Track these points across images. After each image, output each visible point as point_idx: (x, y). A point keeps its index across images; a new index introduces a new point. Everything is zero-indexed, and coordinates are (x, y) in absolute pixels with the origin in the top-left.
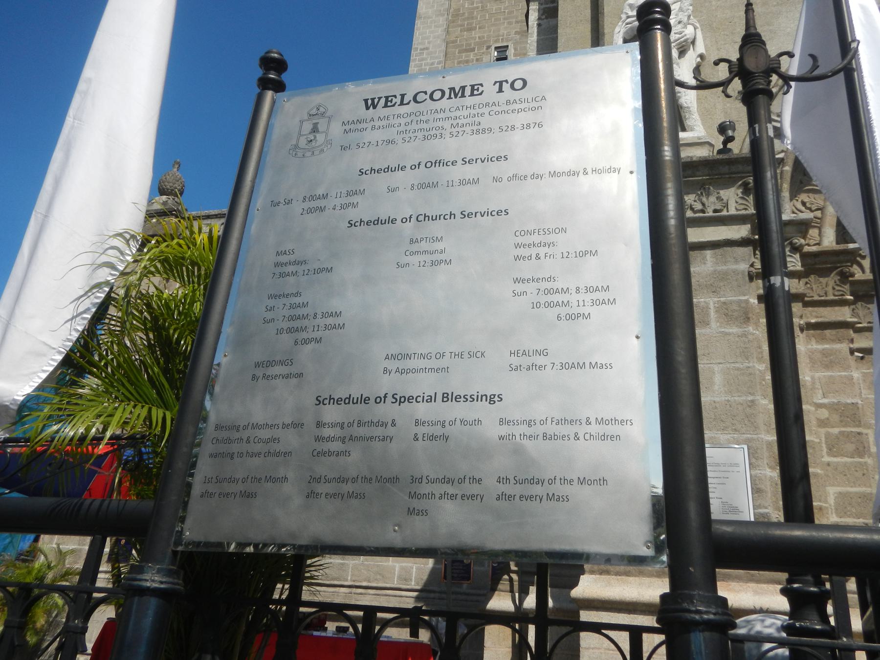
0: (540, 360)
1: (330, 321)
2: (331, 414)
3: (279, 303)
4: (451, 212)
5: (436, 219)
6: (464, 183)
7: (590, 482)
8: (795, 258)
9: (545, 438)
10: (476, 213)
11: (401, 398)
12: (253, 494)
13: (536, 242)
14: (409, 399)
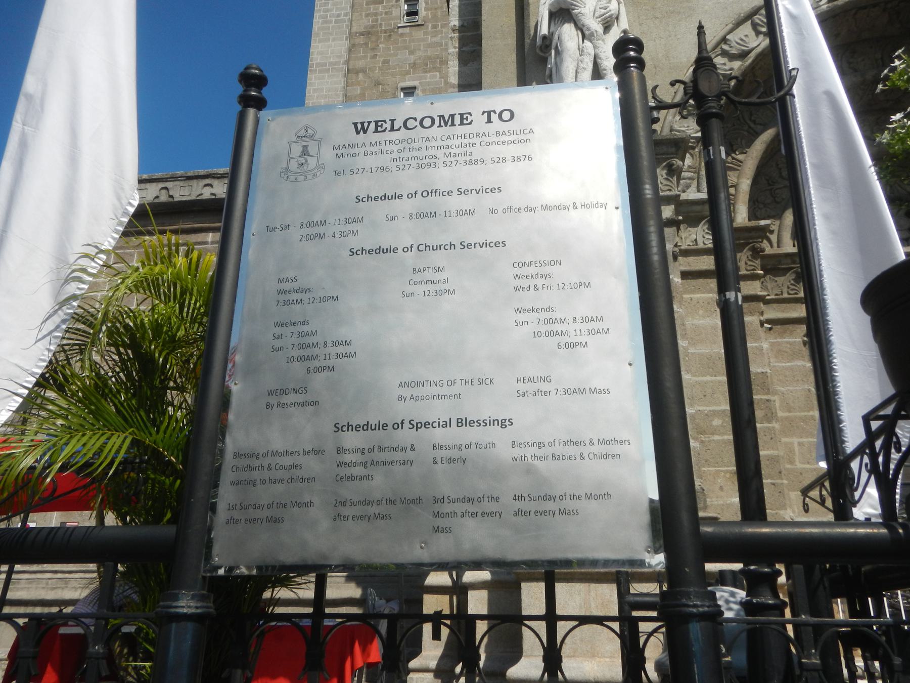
0: (544, 386)
1: (341, 349)
2: (351, 440)
3: (287, 330)
4: (451, 243)
7: (597, 497)
9: (554, 459)
10: (475, 244)
11: (417, 423)
12: (280, 519)
13: (534, 273)
14: (425, 425)
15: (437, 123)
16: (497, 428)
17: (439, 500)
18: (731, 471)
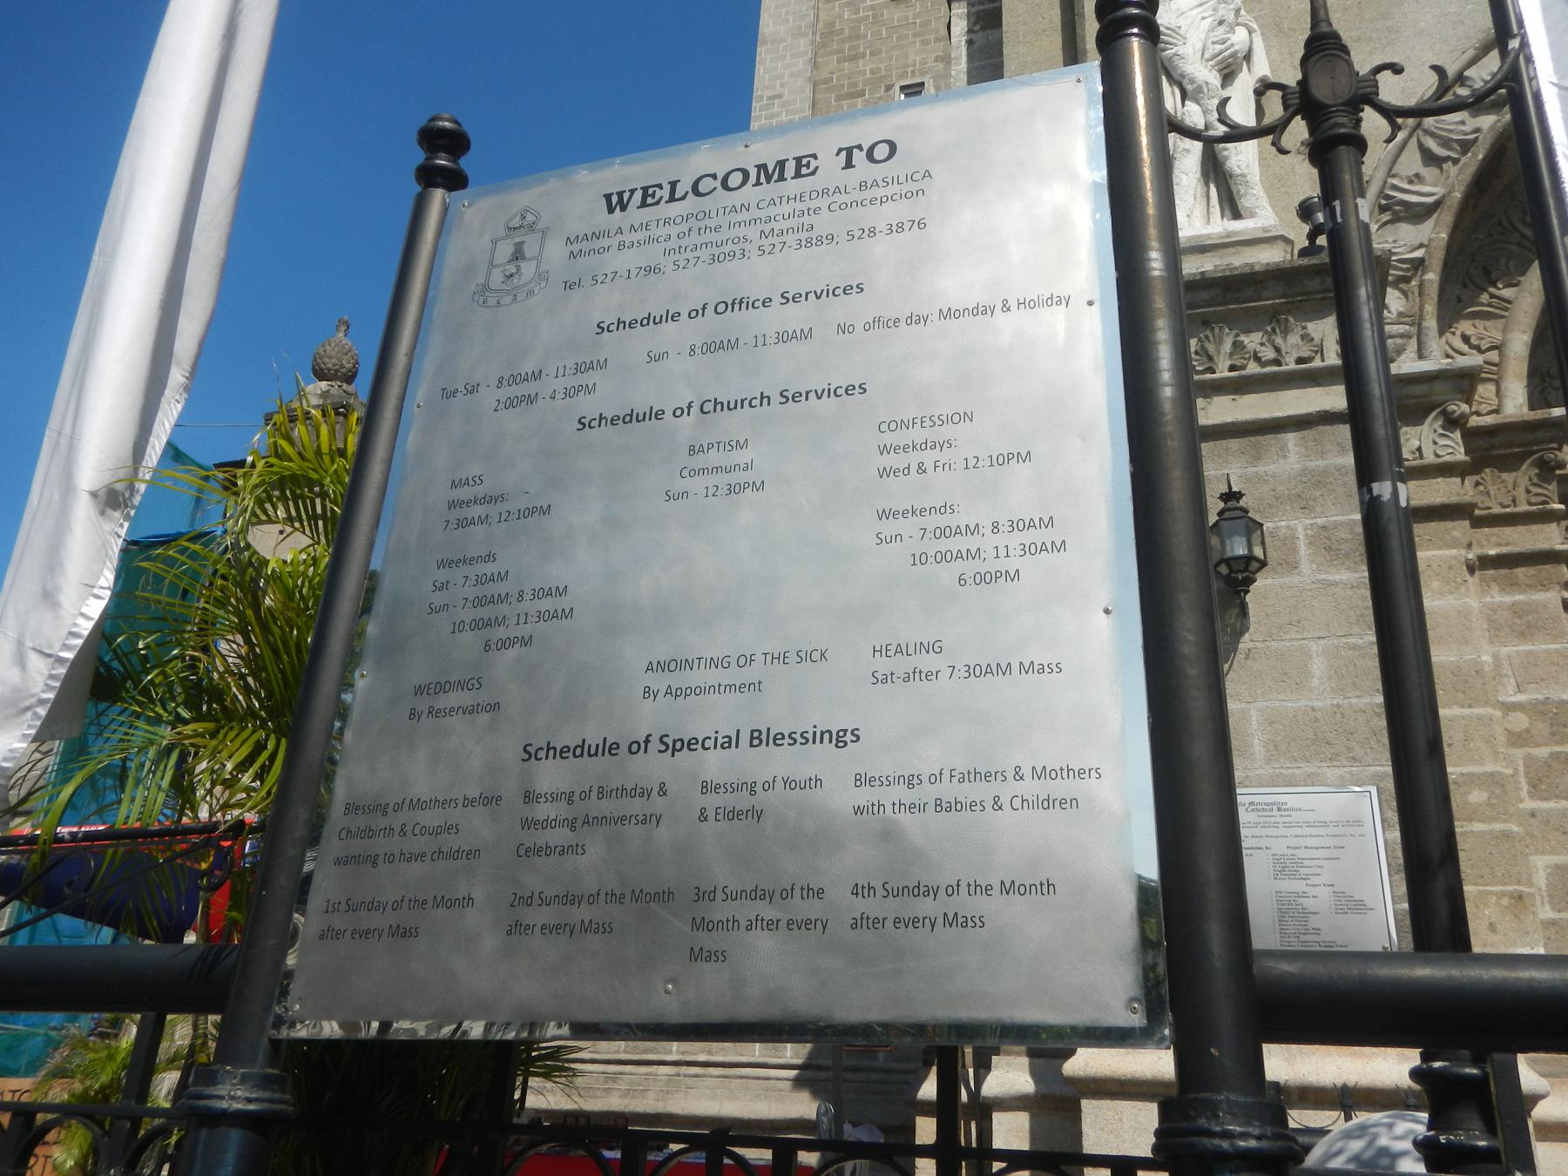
0: (927, 662)
1: (546, 604)
2: (551, 776)
3: (457, 574)
4: (762, 393)
5: (735, 407)
6: (785, 339)
7: (1025, 890)
8: (1453, 440)
9: (939, 809)
10: (807, 393)
11: (675, 742)
12: (413, 930)
13: (919, 441)
14: (689, 744)
15: (753, 179)
16: (828, 747)
17: (707, 894)
18: (1511, 892)
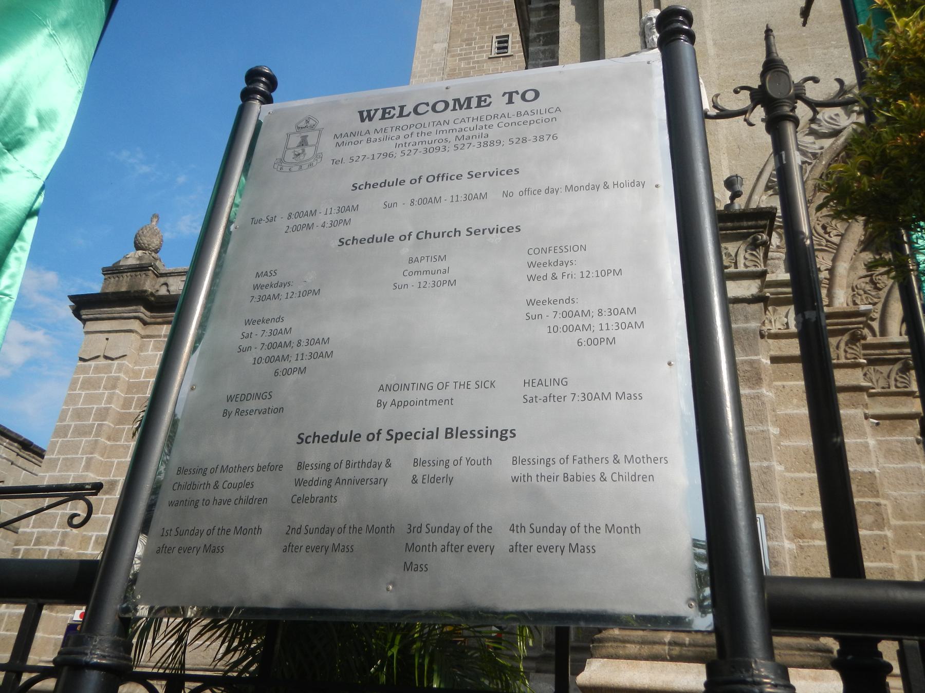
0: (558, 390)
2: (314, 453)
4: (455, 229)
5: (439, 236)
7: (621, 530)
9: (566, 479)
10: (484, 230)
11: (397, 434)
13: (553, 260)
15: (451, 107)
16: (495, 440)
17: (416, 529)
